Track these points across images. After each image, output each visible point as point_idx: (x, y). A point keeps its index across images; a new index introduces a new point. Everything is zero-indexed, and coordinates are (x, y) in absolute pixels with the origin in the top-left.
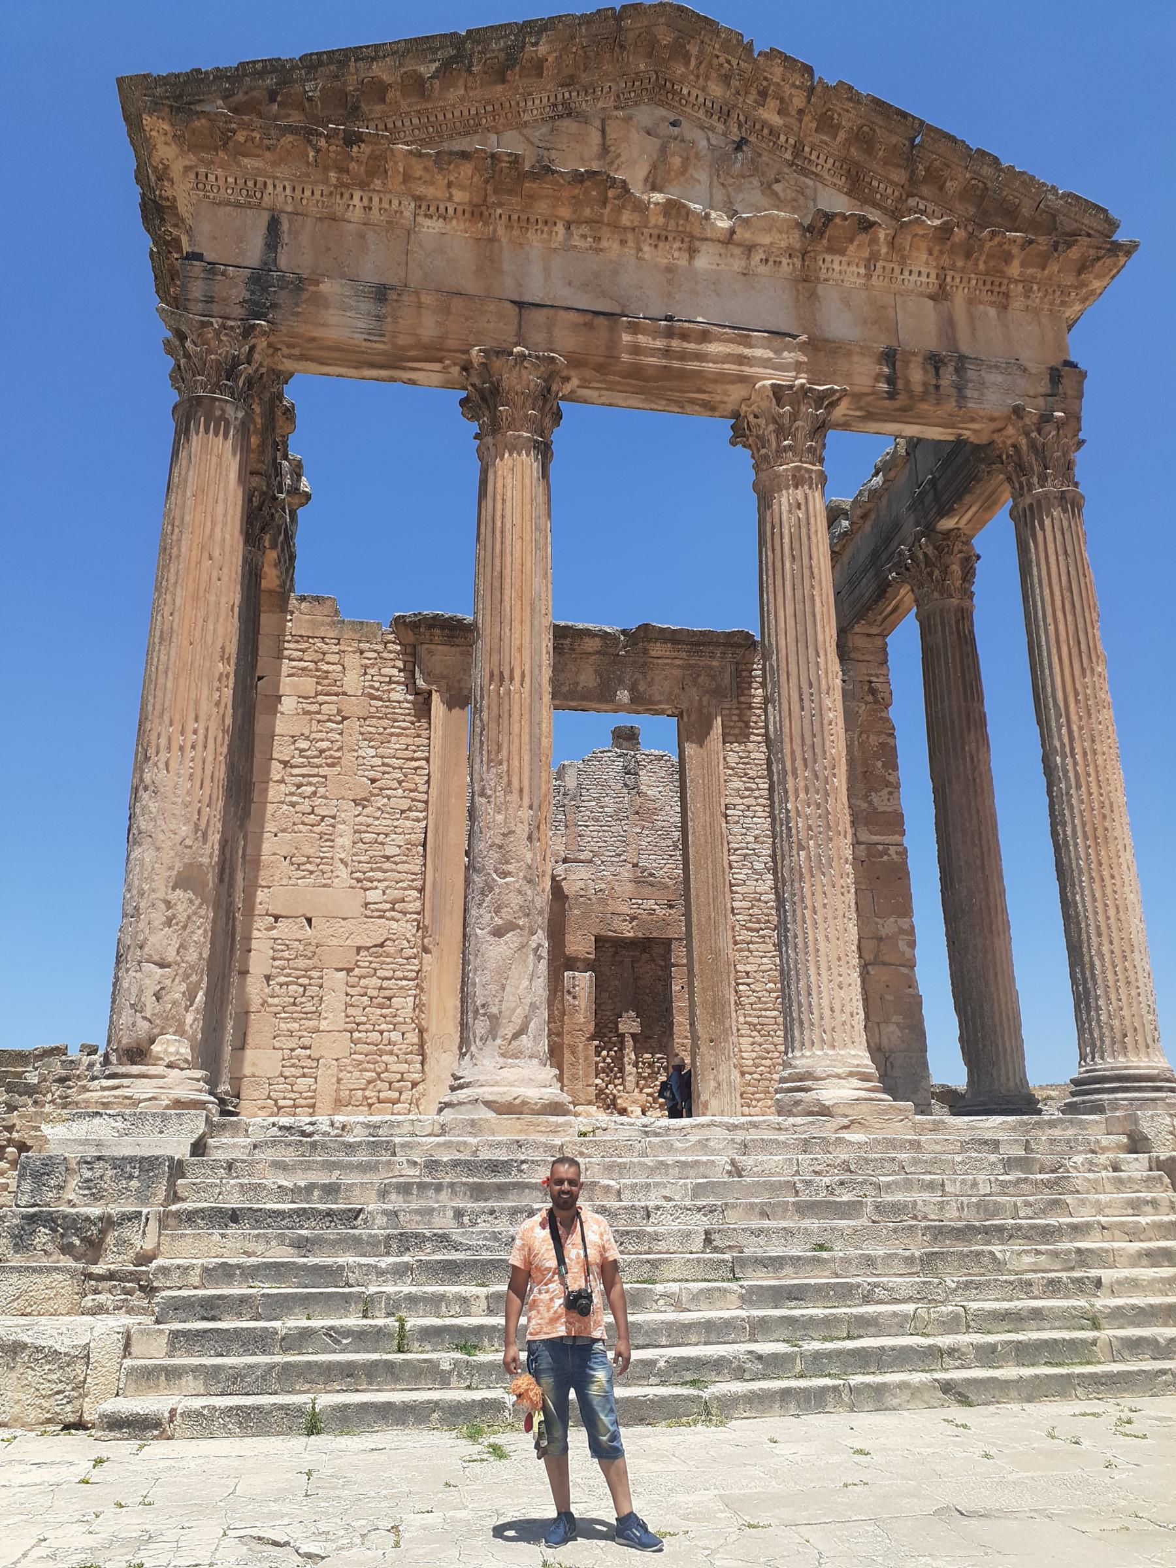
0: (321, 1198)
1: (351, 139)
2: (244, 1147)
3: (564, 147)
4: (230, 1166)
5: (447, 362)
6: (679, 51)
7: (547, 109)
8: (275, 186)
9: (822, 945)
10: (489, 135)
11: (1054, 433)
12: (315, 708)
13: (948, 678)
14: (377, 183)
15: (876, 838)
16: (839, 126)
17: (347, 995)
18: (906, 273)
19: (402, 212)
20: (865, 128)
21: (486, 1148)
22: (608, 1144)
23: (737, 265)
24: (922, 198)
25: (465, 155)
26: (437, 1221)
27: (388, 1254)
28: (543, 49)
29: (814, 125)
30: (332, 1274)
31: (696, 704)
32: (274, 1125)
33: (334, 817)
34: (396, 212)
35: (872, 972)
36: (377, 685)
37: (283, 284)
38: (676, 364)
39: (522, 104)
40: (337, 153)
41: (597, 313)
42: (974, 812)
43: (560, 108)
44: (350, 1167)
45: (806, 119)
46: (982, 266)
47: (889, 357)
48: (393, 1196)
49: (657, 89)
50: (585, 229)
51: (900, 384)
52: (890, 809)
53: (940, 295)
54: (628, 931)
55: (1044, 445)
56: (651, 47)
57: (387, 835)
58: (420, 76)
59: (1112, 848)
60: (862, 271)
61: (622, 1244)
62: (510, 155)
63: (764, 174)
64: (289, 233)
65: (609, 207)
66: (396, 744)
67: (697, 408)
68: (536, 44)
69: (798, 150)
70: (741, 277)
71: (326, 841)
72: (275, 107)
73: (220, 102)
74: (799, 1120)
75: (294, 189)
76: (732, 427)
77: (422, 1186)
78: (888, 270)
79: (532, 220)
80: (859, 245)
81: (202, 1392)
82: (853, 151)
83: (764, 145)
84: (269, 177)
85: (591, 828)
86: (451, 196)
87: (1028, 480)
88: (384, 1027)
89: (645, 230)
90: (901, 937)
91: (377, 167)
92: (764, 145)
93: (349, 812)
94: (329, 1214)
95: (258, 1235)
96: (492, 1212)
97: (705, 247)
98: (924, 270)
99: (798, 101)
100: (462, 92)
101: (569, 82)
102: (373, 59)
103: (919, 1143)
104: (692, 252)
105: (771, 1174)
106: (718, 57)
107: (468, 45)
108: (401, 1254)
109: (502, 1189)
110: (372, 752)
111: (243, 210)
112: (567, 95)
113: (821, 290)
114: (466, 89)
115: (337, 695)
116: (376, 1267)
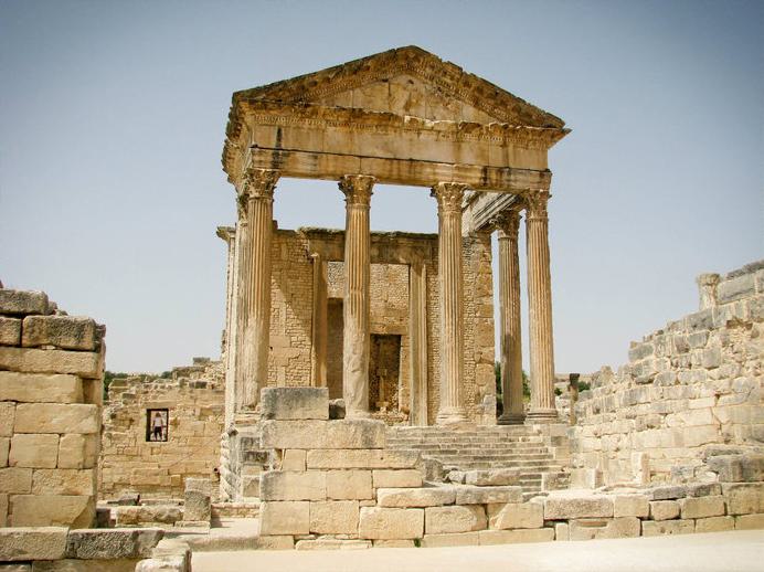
1: (307, 106)
6: (416, 58)
23: (435, 137)
28: (369, 64)
41: (387, 159)
53: (504, 145)
54: (382, 331)
56: (407, 58)
66: (300, 280)
69: (457, 92)
82: (476, 93)
91: (315, 112)
97: (423, 132)
99: (457, 76)
104: (419, 134)
113: (463, 145)
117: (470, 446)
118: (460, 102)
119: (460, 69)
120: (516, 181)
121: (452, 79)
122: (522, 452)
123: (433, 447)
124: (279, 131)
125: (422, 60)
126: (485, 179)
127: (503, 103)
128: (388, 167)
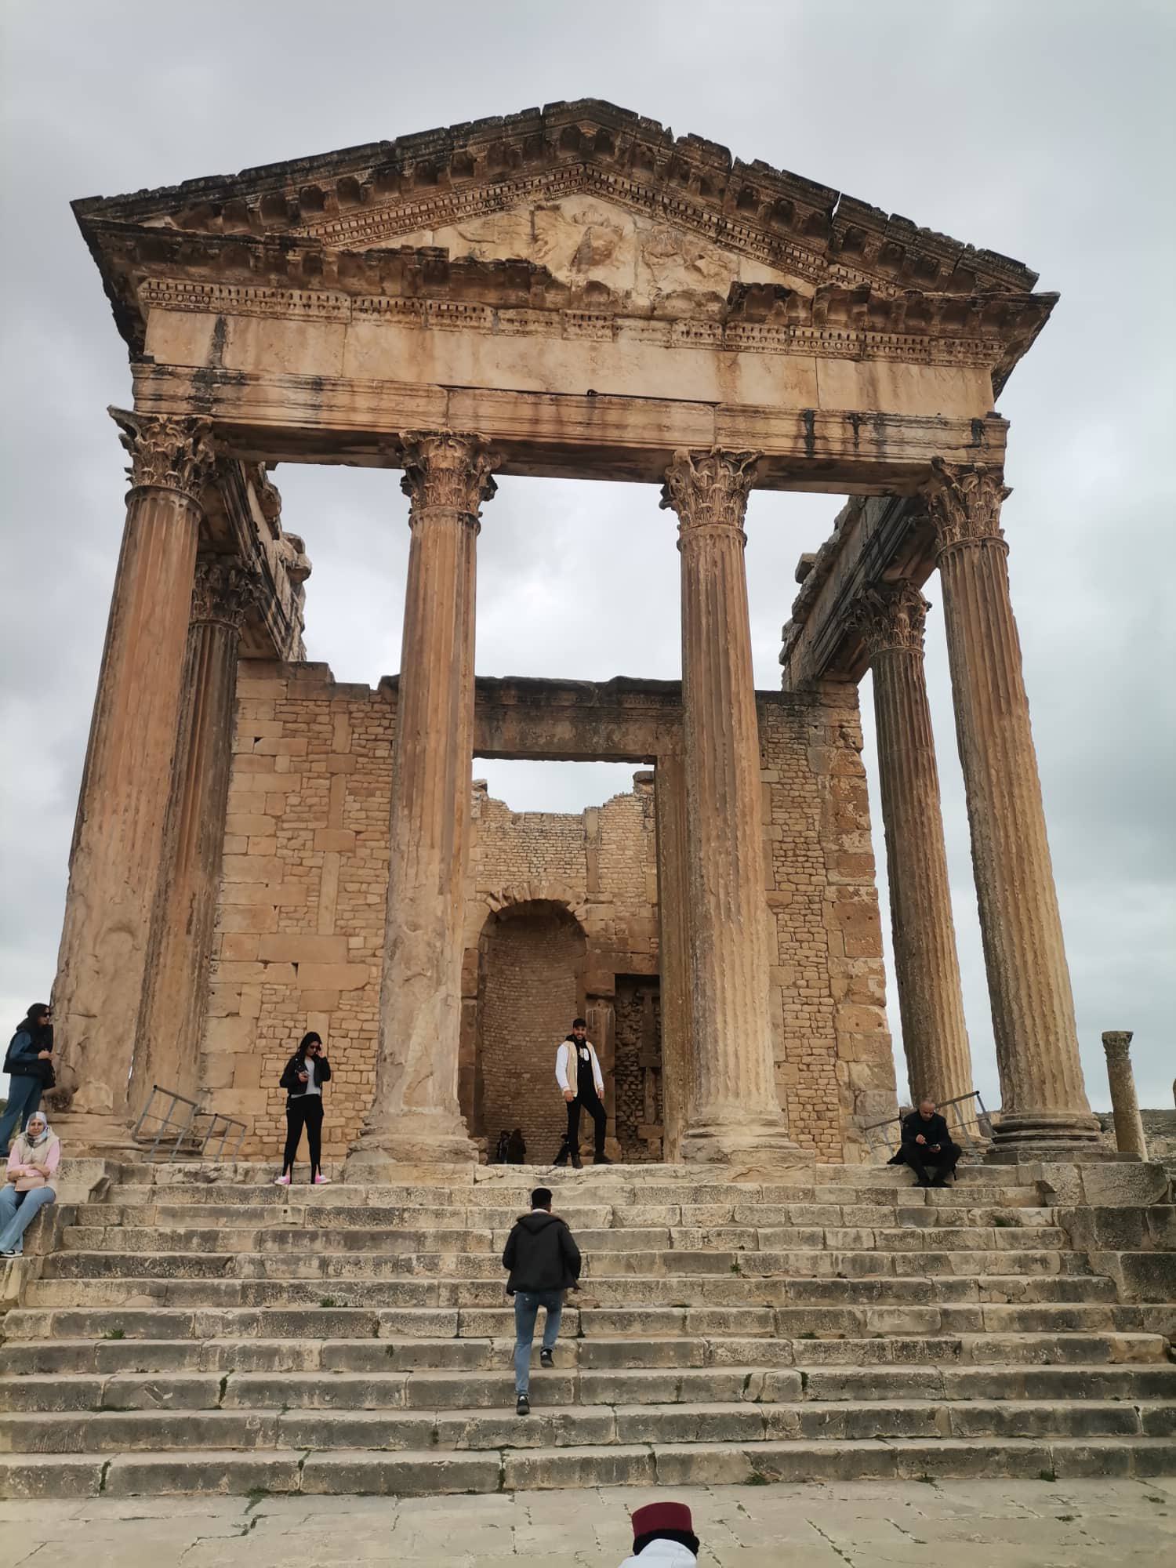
0: (199, 1245)
1: (289, 244)
2: (143, 1193)
3: (495, 239)
4: (123, 1212)
5: (382, 445)
6: (603, 143)
7: (480, 205)
8: (221, 291)
9: (729, 994)
10: (423, 232)
11: (975, 482)
12: (307, 766)
13: (897, 722)
14: (315, 281)
15: (847, 880)
16: (758, 202)
17: (329, 1035)
18: (826, 335)
19: (339, 308)
20: (783, 202)
21: (377, 1195)
22: (496, 1192)
24: (843, 265)
25: (392, 252)
26: (303, 1270)
27: (244, 1304)
28: (472, 149)
29: (735, 203)
30: (178, 1325)
31: (669, 752)
32: (180, 1171)
33: (320, 868)
34: (334, 308)
35: (842, 1012)
36: (363, 743)
37: (226, 379)
38: (596, 433)
39: (455, 201)
40: (273, 257)
42: (921, 855)
43: (492, 202)
44: (237, 1214)
45: (726, 198)
46: (902, 326)
47: (808, 417)
48: (269, 1245)
49: (585, 180)
50: (511, 314)
51: (819, 445)
52: (860, 851)
55: (965, 495)
57: (369, 883)
58: (356, 182)
59: (1030, 893)
60: (782, 336)
61: (477, 1296)
62: (435, 249)
63: (688, 252)
64: (235, 331)
65: (533, 290)
67: (624, 475)
68: (465, 146)
70: (663, 349)
71: (314, 890)
72: (220, 220)
73: (168, 219)
74: (696, 1168)
75: (238, 292)
76: (662, 492)
77: (298, 1235)
78: (808, 334)
79: (461, 309)
80: (779, 314)
81: (9, 1448)
82: (773, 224)
83: (688, 225)
84: (215, 283)
85: (611, 870)
86: (383, 288)
87: (951, 530)
88: (362, 1067)
89: (569, 312)
90: (872, 976)
91: (314, 265)
92: (688, 225)
93: (333, 862)
94: (199, 1263)
95: (120, 1285)
96: (357, 1263)
97: (627, 322)
98: (844, 335)
100: (397, 195)
101: (501, 178)
102: (309, 170)
103: (813, 1192)
104: (616, 330)
105: (654, 1225)
106: (640, 146)
107: (398, 152)
108: (257, 1304)
109: (375, 1238)
110: (357, 806)
111: (193, 315)
112: (498, 191)
114: (400, 192)
115: (327, 753)
116: (222, 1318)
117: (788, 1239)
118: (733, 256)
119: (725, 151)
120: (902, 442)
121: (705, 188)
122: (984, 1266)
123: (648, 1239)
124: (220, 328)
125: (618, 142)
126: (810, 438)
127: (853, 243)
128: (526, 411)
